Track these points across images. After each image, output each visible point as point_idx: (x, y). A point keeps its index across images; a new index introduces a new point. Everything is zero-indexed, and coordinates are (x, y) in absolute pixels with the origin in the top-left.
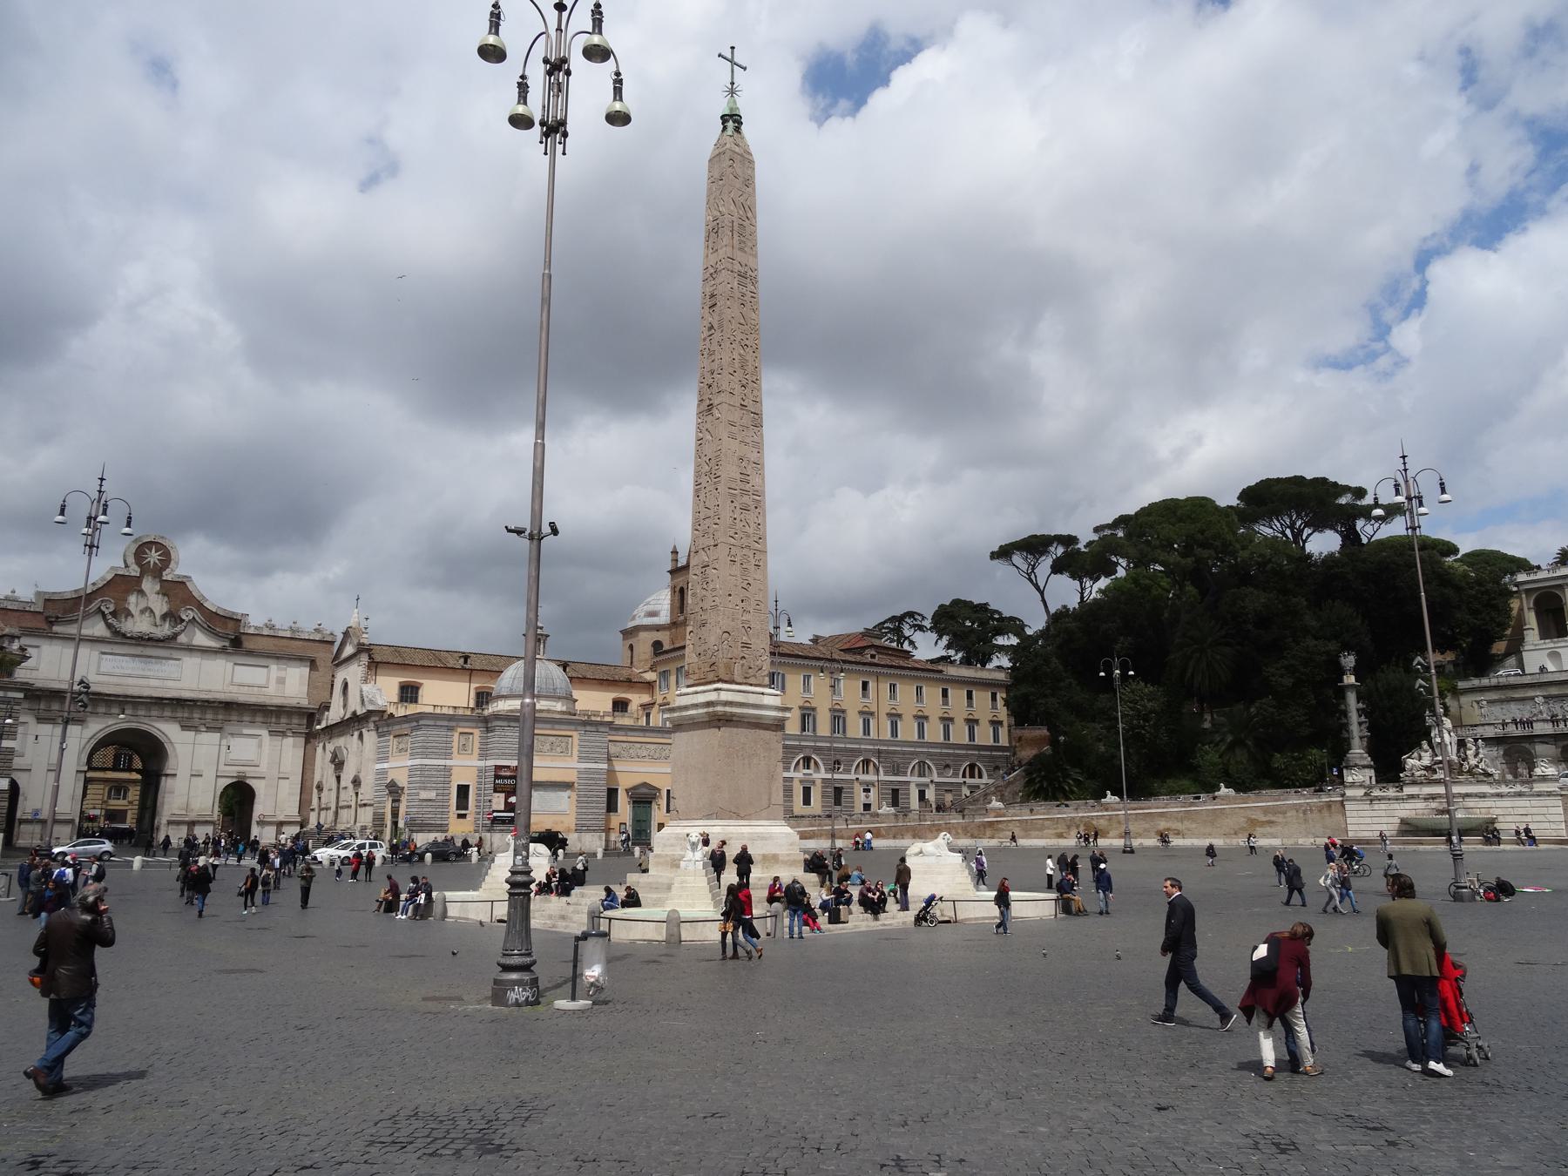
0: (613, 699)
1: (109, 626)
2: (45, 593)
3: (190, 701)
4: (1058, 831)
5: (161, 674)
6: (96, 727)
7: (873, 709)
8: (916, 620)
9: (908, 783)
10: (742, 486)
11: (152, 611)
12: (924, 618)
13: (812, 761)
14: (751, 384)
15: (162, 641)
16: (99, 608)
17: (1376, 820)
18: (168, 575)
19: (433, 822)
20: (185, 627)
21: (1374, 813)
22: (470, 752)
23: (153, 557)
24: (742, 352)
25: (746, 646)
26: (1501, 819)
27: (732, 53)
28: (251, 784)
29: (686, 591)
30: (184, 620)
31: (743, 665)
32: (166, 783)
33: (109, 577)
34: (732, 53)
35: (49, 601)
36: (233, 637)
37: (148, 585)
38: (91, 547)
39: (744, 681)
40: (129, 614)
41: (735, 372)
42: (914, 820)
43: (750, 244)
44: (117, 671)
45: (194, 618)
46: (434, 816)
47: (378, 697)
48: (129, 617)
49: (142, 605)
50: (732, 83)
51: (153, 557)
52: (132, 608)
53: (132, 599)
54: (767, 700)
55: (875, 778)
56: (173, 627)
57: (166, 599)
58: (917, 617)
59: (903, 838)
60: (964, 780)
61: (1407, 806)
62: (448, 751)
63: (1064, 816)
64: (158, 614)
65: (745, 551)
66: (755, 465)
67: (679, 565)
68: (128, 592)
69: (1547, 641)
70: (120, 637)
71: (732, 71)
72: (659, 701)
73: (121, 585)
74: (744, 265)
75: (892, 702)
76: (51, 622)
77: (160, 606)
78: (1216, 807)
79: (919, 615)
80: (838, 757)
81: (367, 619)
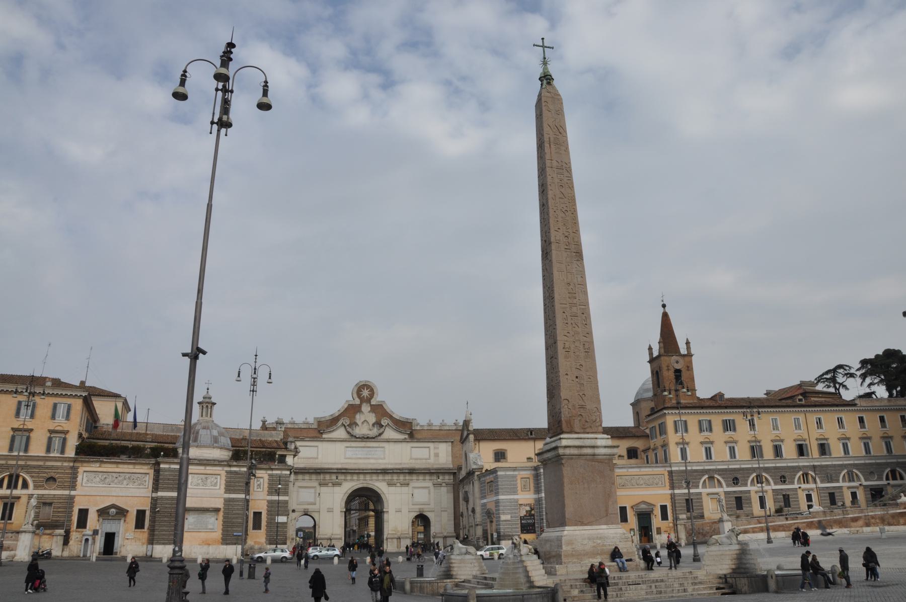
0: (627, 449)
1: (348, 433)
2: (318, 418)
3: (391, 470)
5: (375, 456)
6: (349, 485)
8: (845, 370)
9: (841, 488)
10: (571, 302)
11: (367, 422)
12: (850, 367)
13: (764, 477)
14: (572, 234)
15: (374, 438)
16: (343, 423)
18: (373, 402)
19: (511, 534)
20: (385, 429)
22: (528, 489)
23: (365, 393)
24: (563, 215)
25: (582, 407)
27: (543, 42)
28: (427, 515)
29: (659, 373)
30: (383, 426)
31: (580, 420)
32: (386, 516)
33: (346, 406)
34: (543, 42)
35: (320, 423)
36: (409, 432)
37: (366, 408)
38: (253, 391)
39: (582, 431)
40: (356, 424)
41: (559, 229)
42: (839, 515)
43: (563, 148)
44: (354, 456)
45: (388, 424)
46: (511, 530)
47: (478, 460)
48: (357, 427)
49: (363, 420)
50: (545, 58)
51: (365, 393)
52: (357, 421)
53: (358, 416)
54: (599, 443)
55: (812, 486)
56: (379, 430)
57: (374, 415)
58: (847, 368)
60: (888, 482)
62: (515, 490)
64: (371, 424)
65: (577, 344)
66: (580, 286)
67: (654, 356)
68: (356, 413)
70: (353, 437)
71: (544, 52)
72: (652, 447)
73: (352, 410)
74: (560, 161)
75: (820, 431)
76: (322, 433)
77: (372, 418)
79: (846, 366)
80: (783, 474)
81: (471, 414)
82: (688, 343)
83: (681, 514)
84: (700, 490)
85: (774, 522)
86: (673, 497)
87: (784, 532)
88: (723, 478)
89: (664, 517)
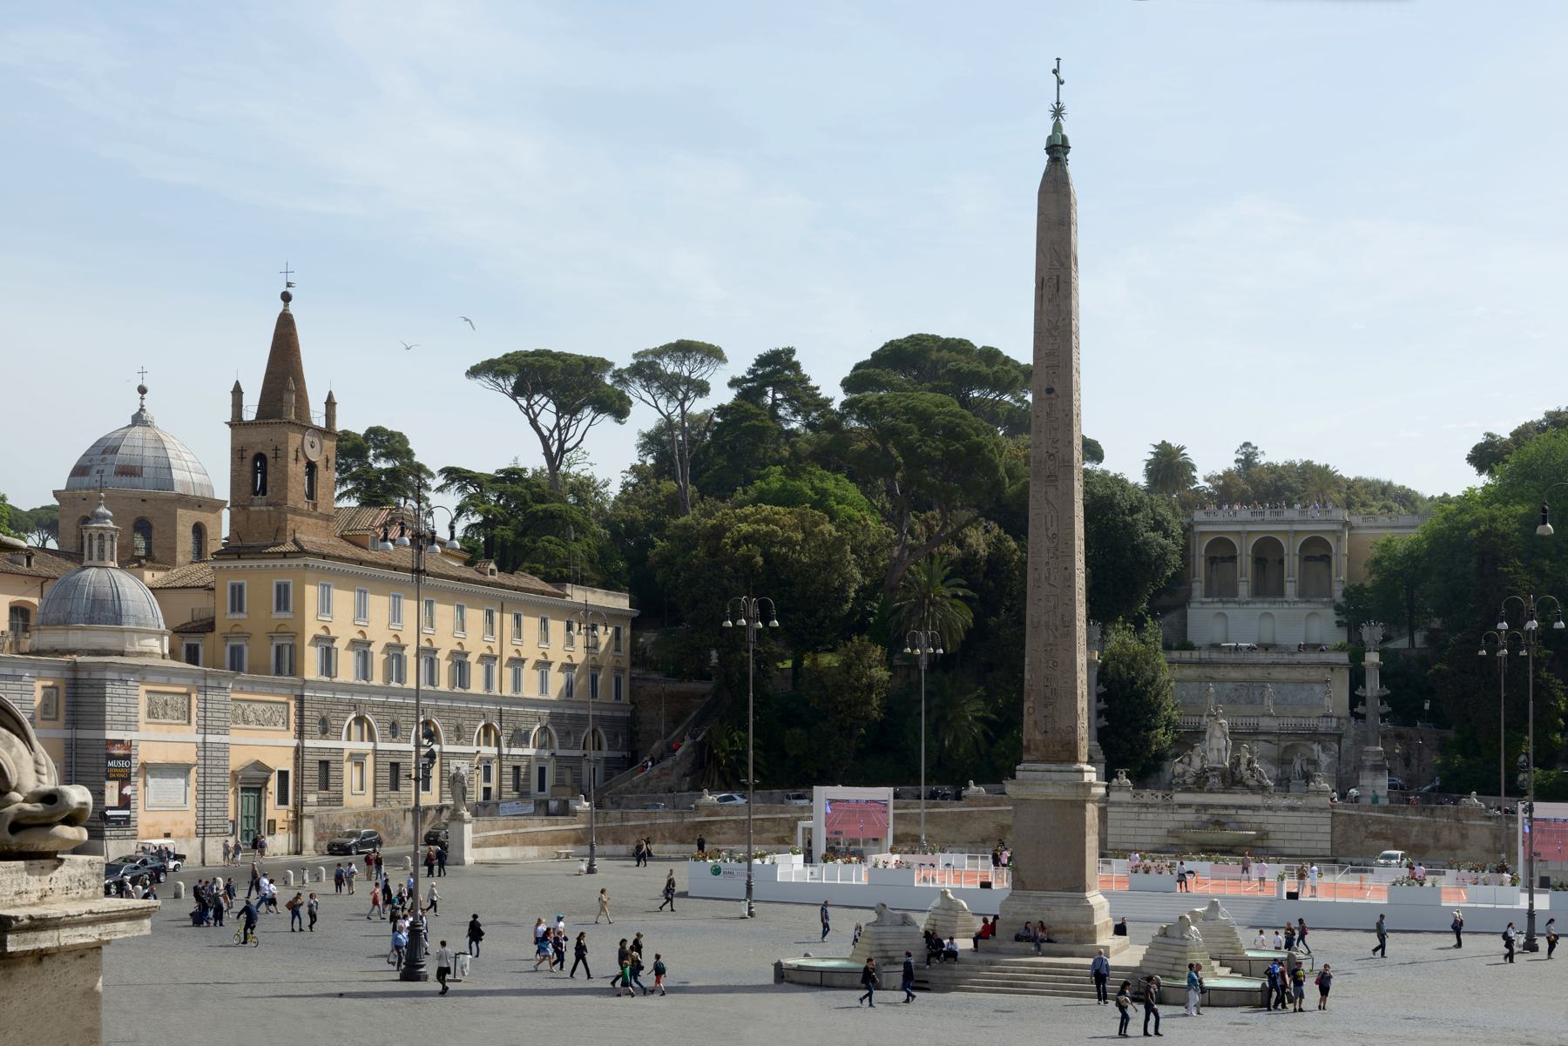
4: (781, 834)
7: (496, 652)
17: (1140, 831)
21: (1141, 824)
26: (1271, 835)
42: (616, 820)
59: (603, 844)
61: (1177, 817)
63: (788, 815)
69: (1216, 600)
78: (963, 809)
82: (330, 403)
83: (311, 792)
84: (342, 744)
85: (525, 827)
86: (299, 752)
87: (536, 847)
88: (378, 721)
89: (283, 800)
